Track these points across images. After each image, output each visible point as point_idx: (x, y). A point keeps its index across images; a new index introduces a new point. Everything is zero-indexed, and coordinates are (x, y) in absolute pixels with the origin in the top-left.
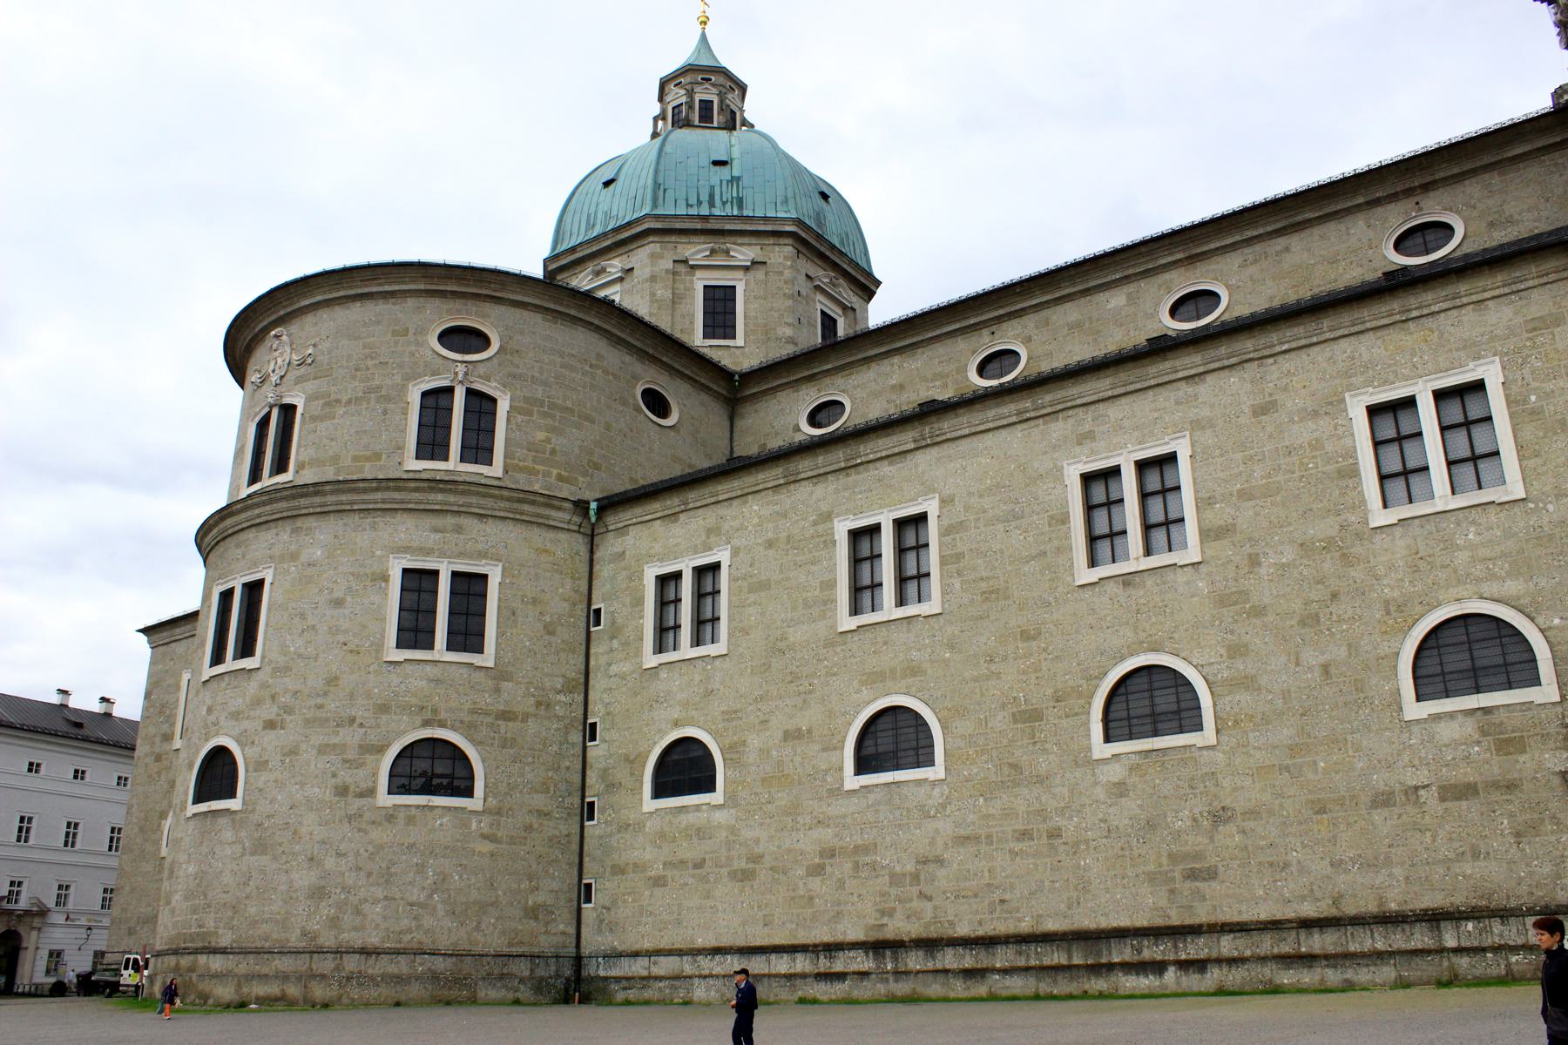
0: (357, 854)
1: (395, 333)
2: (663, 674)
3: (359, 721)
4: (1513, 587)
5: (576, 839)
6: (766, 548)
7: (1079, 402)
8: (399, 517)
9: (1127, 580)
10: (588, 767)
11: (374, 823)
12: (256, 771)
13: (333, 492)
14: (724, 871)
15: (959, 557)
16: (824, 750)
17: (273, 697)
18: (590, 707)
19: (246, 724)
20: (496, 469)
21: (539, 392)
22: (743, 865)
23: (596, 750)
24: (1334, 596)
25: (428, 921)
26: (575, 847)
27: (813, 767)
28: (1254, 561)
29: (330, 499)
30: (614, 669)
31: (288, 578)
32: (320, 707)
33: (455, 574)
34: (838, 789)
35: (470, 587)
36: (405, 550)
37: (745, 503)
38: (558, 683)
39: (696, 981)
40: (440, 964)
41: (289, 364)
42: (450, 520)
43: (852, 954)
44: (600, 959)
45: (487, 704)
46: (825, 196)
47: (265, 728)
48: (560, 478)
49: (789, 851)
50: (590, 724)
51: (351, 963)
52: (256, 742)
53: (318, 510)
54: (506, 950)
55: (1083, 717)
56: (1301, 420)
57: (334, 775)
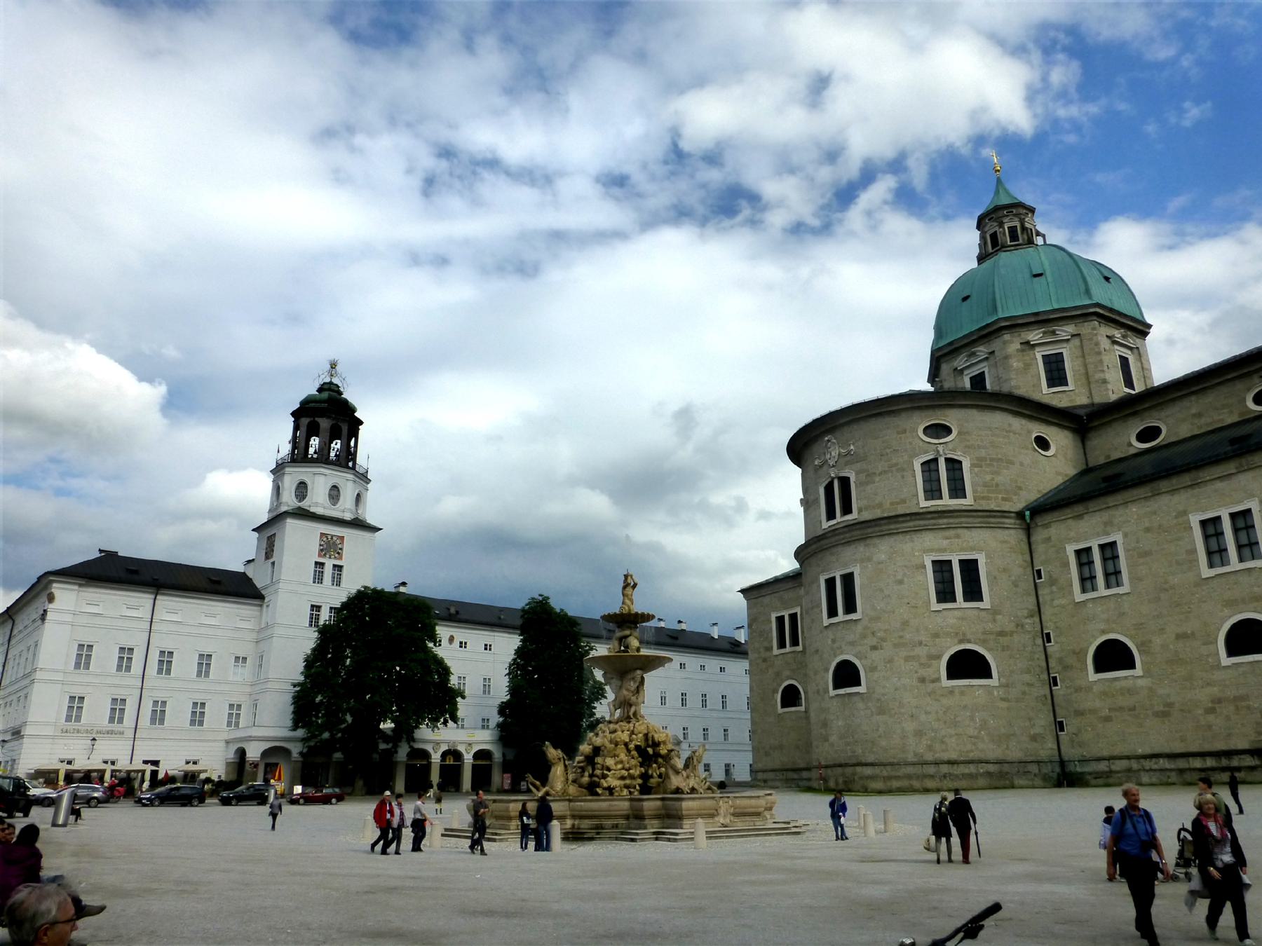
0: (937, 712)
1: (898, 433)
3: (924, 643)
5: (1049, 697)
10: (1049, 657)
12: (871, 671)
13: (885, 524)
14: (1149, 712)
16: (1204, 644)
17: (873, 633)
18: (1044, 624)
19: (859, 648)
20: (967, 502)
21: (983, 453)
22: (1161, 708)
23: (1052, 647)
25: (981, 746)
26: (1049, 701)
30: (1056, 602)
32: (901, 637)
33: (960, 561)
34: (1218, 665)
35: (969, 568)
36: (932, 550)
37: (1127, 507)
38: (1025, 613)
39: (1142, 773)
40: (991, 768)
41: (839, 455)
42: (952, 532)
43: (1242, 757)
44: (1076, 762)
46: (1107, 279)
47: (871, 650)
48: (1003, 499)
50: (1046, 634)
51: (945, 769)
53: (879, 534)
54: (1024, 759)
57: (916, 672)
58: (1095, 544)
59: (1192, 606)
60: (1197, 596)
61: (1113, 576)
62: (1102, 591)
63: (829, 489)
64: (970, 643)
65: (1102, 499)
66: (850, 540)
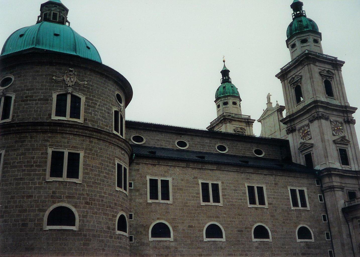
2: (153, 205)
9: (256, 209)
13: (104, 134)
15: (225, 195)
28: (276, 210)
37: (175, 168)
58: (159, 179)
59: (196, 215)
60: (198, 211)
61: (166, 196)
62: (160, 200)
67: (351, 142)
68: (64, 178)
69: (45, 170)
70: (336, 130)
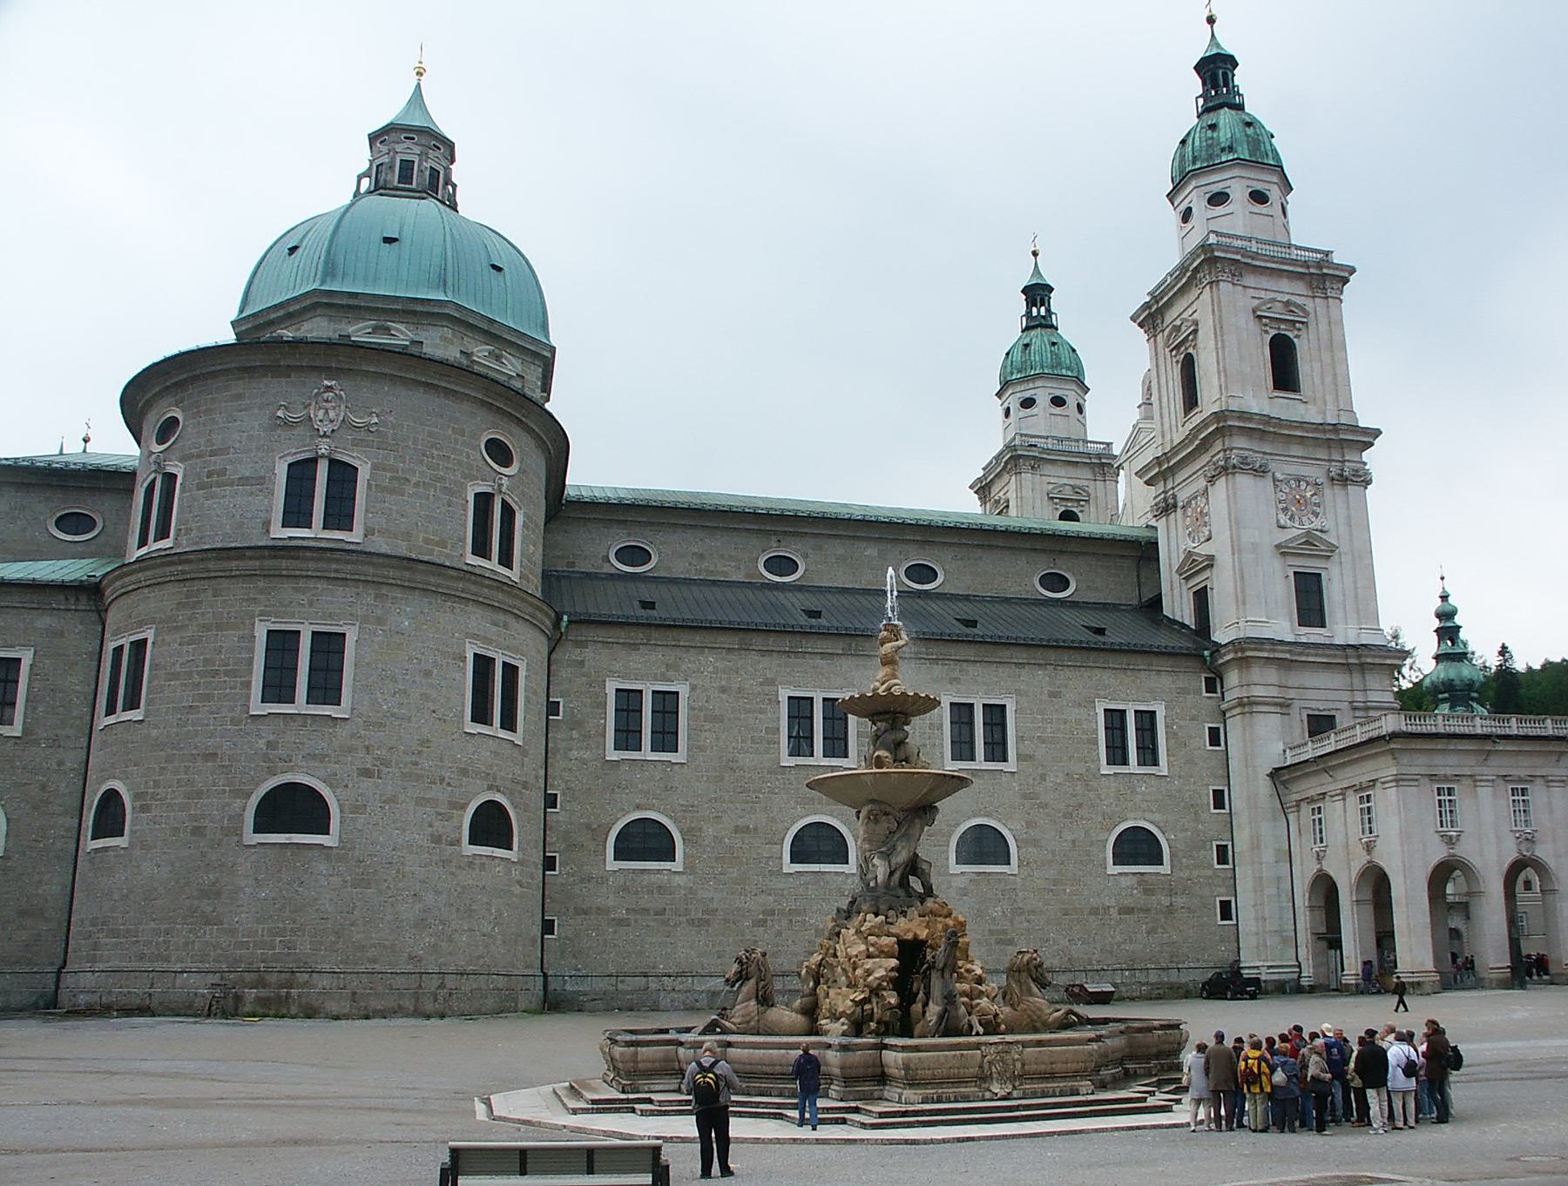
4: (1157, 817)
6: (720, 692)
7: (953, 658)
8: (471, 608)
11: (460, 867)
22: (700, 915)
24: (1080, 805)
27: (759, 854)
28: (1043, 777)
29: (419, 577)
31: (376, 639)
36: (476, 636)
41: (343, 420)
42: (501, 617)
45: (519, 776)
49: (738, 909)
52: (350, 785)
53: (406, 584)
55: (945, 848)
56: (1073, 706)
58: (648, 689)
61: (666, 738)
62: (647, 753)
63: (301, 473)
64: (499, 791)
65: (675, 632)
66: (348, 576)
67: (1344, 547)
68: (301, 704)
69: (248, 685)
70: (1294, 505)
